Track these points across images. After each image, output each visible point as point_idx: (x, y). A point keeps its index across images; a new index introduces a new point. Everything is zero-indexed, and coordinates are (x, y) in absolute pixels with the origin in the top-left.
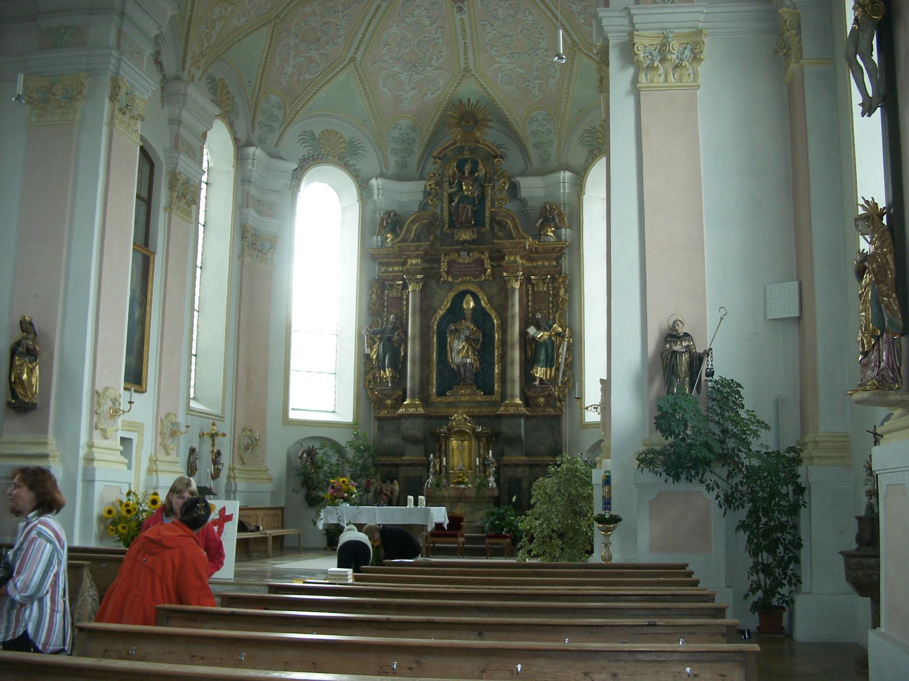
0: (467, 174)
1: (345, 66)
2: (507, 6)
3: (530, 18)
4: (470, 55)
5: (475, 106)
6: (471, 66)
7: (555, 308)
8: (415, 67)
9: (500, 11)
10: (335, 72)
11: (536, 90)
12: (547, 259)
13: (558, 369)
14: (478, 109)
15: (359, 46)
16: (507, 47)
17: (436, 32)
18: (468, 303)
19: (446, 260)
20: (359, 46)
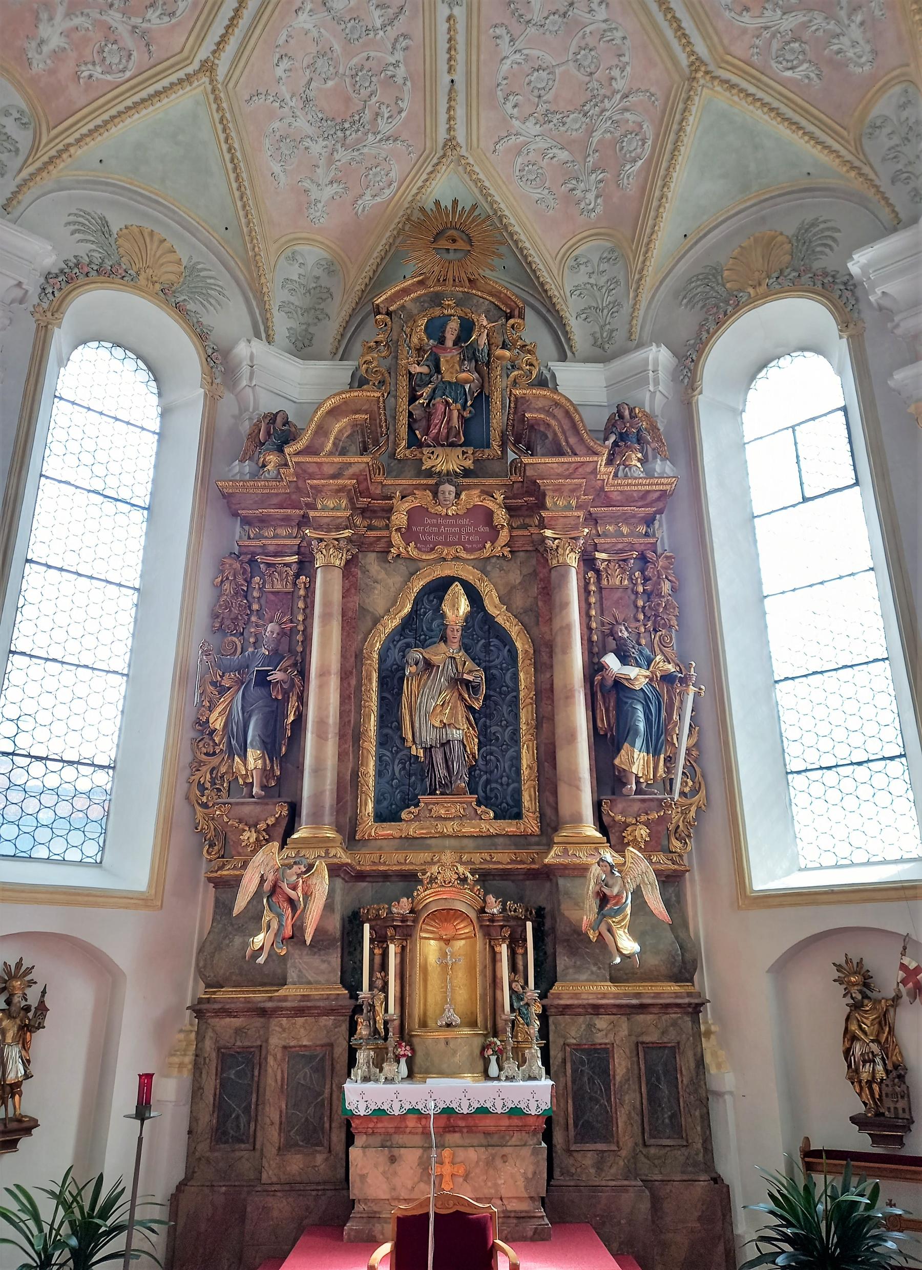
0: (449, 343)
1: (189, 78)
4: (460, 112)
5: (468, 217)
6: (461, 138)
7: (649, 624)
8: (343, 130)
10: (166, 82)
11: (591, 196)
12: (626, 519)
13: (670, 760)
15: (223, 39)
16: (539, 97)
17: (394, 48)
18: (455, 606)
19: (406, 506)
20: (223, 39)
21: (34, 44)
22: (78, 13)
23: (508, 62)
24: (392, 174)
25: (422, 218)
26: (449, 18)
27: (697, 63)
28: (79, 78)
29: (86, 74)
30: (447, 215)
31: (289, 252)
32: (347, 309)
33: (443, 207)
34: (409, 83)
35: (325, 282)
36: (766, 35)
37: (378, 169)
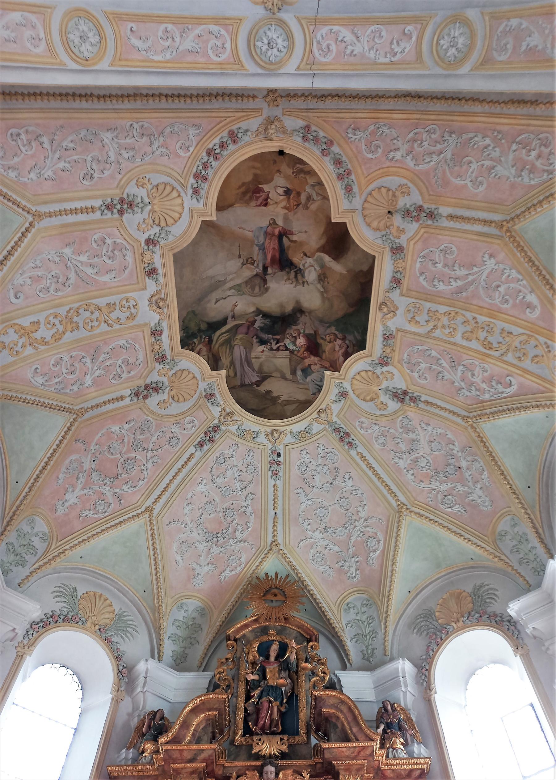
0: (272, 659)
1: (138, 515)
2: (325, 471)
3: (350, 483)
4: (280, 528)
5: (284, 581)
6: (280, 540)
8: (217, 537)
9: (318, 478)
10: (125, 517)
11: (353, 570)
14: (287, 584)
15: (159, 497)
16: (321, 520)
20: (159, 497)
21: (61, 502)
22: (88, 488)
23: (304, 504)
24: (242, 559)
25: (258, 582)
26: (274, 486)
27: (401, 505)
28: (80, 517)
29: (85, 515)
30: (272, 581)
31: (179, 604)
32: (210, 637)
33: (270, 576)
34: (253, 515)
35: (198, 621)
36: (434, 492)
37: (234, 557)
